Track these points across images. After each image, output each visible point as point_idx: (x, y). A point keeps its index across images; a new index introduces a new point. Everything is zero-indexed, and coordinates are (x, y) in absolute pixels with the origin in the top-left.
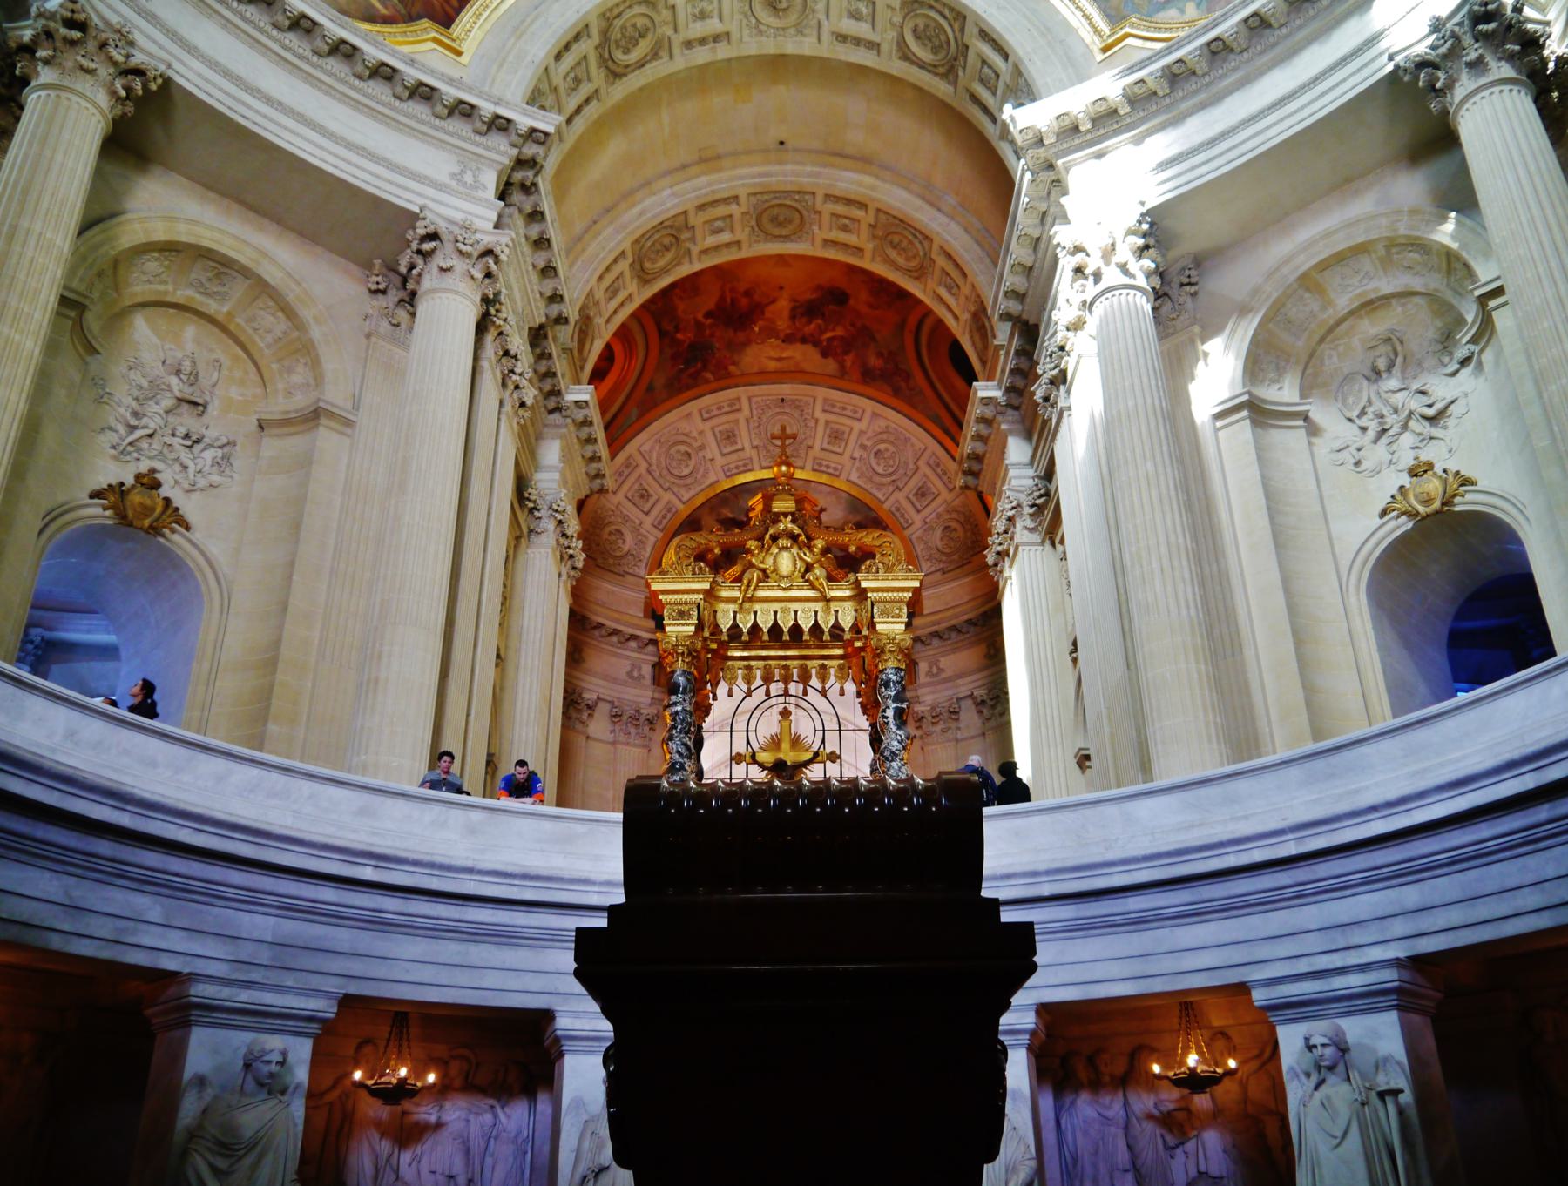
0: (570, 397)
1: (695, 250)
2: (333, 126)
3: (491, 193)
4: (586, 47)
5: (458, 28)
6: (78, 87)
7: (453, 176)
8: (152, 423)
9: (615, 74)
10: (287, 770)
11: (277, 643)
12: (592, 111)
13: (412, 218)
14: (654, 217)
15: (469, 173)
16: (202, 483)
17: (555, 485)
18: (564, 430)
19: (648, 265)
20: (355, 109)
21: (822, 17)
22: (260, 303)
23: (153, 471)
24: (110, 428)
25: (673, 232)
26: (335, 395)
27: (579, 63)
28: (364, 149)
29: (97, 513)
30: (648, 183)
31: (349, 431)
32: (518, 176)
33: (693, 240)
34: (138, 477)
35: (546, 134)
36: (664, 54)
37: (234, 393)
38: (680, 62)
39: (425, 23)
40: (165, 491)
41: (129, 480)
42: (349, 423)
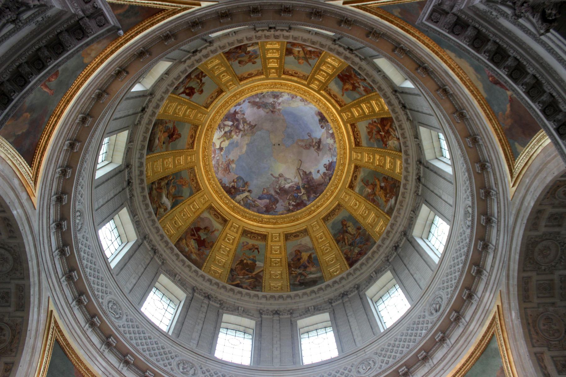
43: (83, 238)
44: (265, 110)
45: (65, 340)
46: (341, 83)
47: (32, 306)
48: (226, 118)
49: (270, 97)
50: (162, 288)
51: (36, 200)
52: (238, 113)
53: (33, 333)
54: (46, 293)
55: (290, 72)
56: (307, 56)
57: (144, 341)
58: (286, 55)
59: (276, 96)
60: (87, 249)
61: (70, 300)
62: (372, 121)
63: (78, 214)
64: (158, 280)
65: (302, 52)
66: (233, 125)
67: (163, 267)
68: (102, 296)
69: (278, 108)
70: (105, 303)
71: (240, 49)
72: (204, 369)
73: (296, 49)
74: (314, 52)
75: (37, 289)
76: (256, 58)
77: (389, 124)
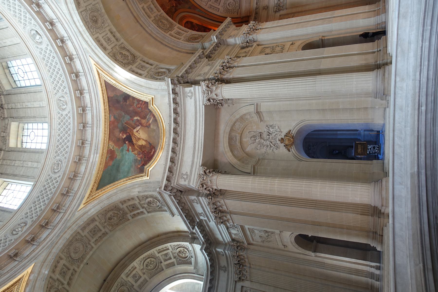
0: (216, 41)
1: (159, 14)
2: (193, 128)
3: (192, 89)
4: (134, 67)
5: (147, 100)
6: (215, 182)
7: (191, 98)
8: (268, 143)
9: (134, 57)
10: (394, 131)
11: (318, 110)
12: (146, 59)
13: (206, 106)
14: (157, 30)
15: (188, 95)
16: (279, 130)
17: (239, 38)
18: (224, 39)
19: (168, 26)
20: (186, 124)
21: (91, 5)
22: (234, 129)
23: (279, 140)
24: (273, 151)
25: (158, 22)
26: (252, 109)
27: (138, 68)
28: (195, 121)
29: (293, 150)
30: (150, 34)
31: (259, 104)
32: (182, 82)
33: (157, 16)
34: (281, 143)
35: (171, 80)
36: (123, 45)
37: (254, 128)
38: (122, 40)
39: (150, 108)
40: (283, 137)
41: (283, 144)
42: (257, 104)
43: (28, 216)
45: (94, 186)
47: (89, 217)
50: (19, 139)
51: (29, 269)
53: (101, 204)
54: (77, 214)
57: (63, 138)
60: (33, 209)
61: (71, 198)
63: (14, 233)
64: (16, 147)
67: (4, 148)
68: (55, 180)
70: (58, 175)
72: (55, 91)
75: (78, 222)
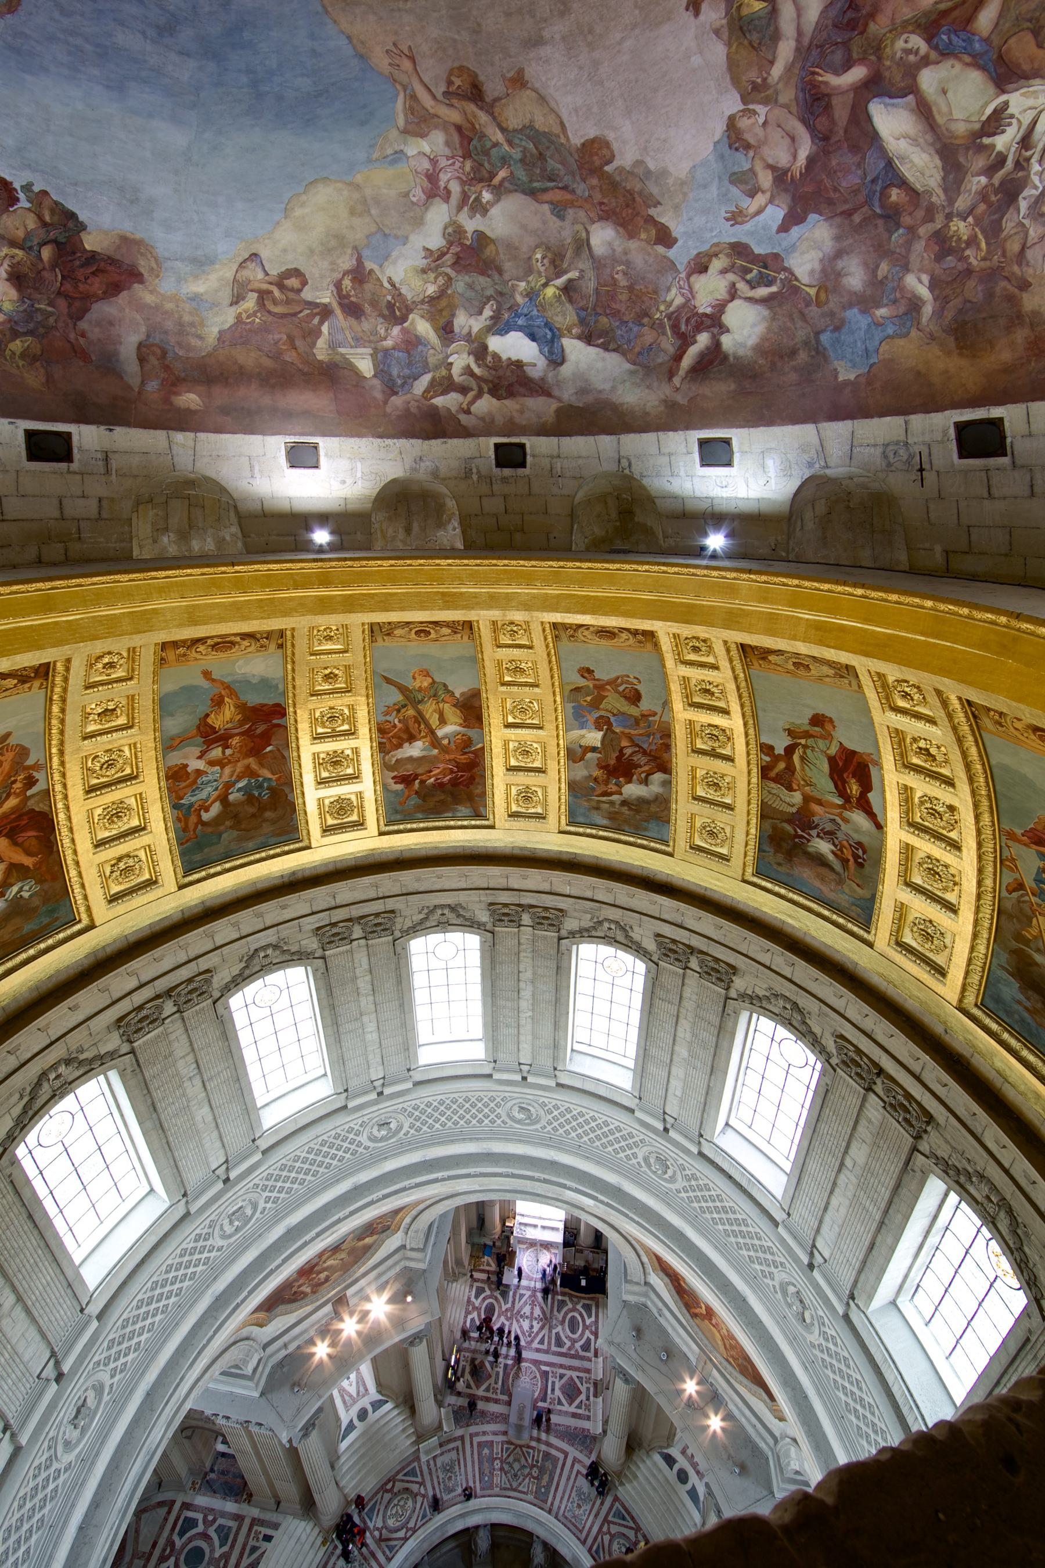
44: (542, 122)
46: (253, 699)
48: (892, 216)
49: (511, 247)
52: (781, 176)
55: (446, 631)
56: (411, 712)
58: (476, 694)
59: (470, 255)
62: (36, 767)
65: (434, 721)
66: (876, 86)
69: (433, 144)
71: (621, 751)
73: (450, 729)
74: (400, 746)
76: (577, 689)
77: (28, 861)
